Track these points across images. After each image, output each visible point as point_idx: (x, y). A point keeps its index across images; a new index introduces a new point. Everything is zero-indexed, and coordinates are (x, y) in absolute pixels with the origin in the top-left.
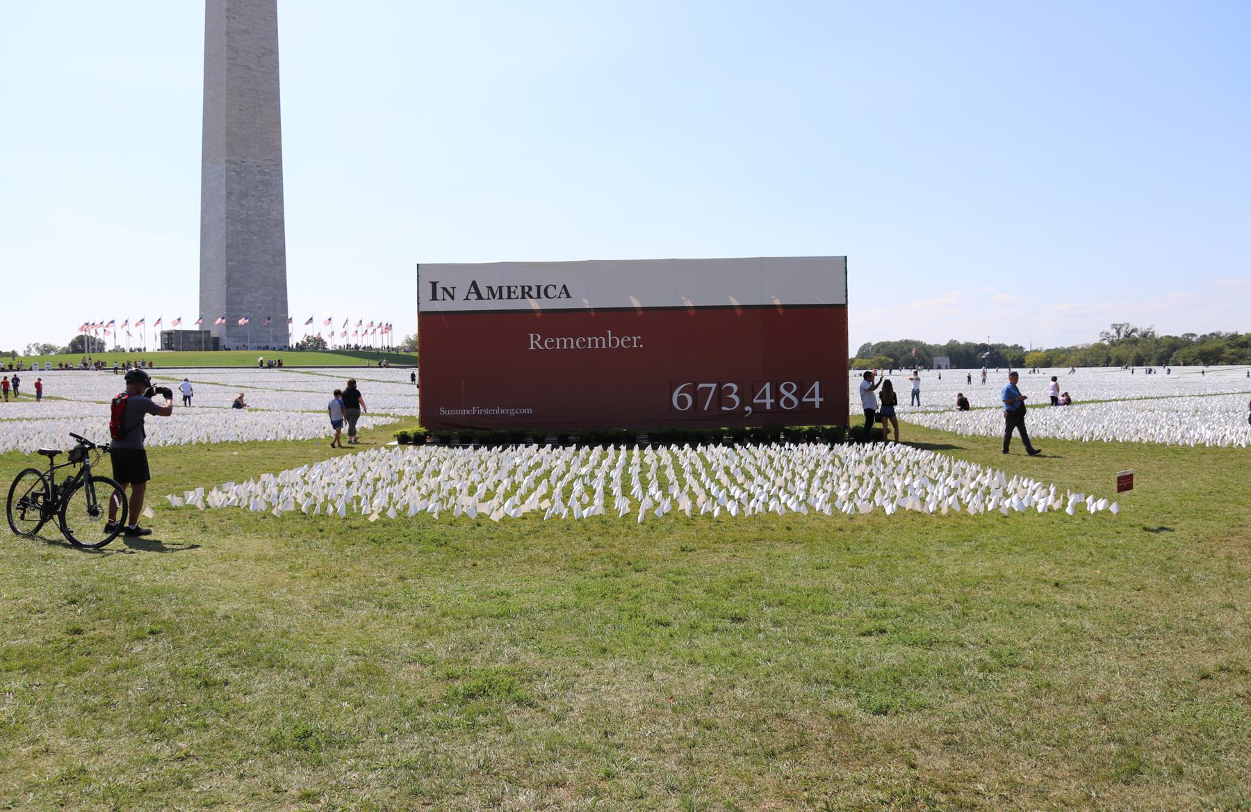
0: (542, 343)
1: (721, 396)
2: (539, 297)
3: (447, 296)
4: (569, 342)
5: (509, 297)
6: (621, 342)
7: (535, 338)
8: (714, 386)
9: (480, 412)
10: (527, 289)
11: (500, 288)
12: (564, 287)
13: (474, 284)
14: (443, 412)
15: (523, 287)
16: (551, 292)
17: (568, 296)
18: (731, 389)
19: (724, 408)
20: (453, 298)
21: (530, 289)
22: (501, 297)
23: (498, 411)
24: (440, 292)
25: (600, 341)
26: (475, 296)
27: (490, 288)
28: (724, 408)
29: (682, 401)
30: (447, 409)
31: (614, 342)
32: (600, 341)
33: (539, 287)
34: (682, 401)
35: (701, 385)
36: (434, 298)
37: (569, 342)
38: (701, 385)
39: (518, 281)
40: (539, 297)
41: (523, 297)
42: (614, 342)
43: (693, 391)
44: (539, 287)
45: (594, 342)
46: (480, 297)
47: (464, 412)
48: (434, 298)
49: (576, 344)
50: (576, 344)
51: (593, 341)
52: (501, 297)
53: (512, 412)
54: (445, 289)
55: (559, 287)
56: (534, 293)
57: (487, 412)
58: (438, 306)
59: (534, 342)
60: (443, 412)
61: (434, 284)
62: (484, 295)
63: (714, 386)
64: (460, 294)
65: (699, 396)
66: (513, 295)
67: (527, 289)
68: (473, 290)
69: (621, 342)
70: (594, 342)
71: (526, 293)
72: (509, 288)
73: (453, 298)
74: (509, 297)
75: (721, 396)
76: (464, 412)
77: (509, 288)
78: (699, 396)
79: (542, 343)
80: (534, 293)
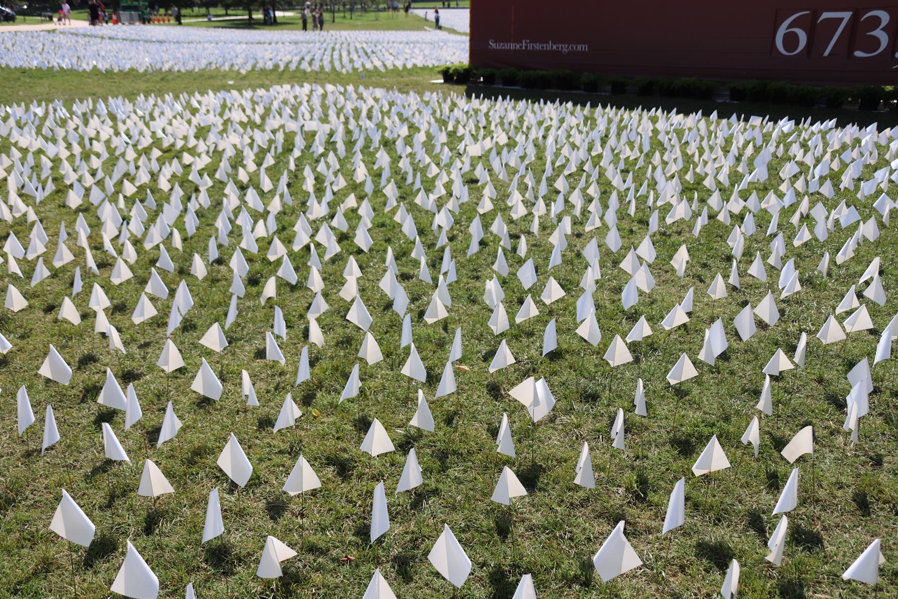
1: (857, 33)
8: (847, 15)
9: (530, 47)
14: (493, 45)
18: (877, 21)
19: (858, 54)
23: (550, 46)
28: (858, 54)
29: (791, 40)
30: (496, 42)
34: (791, 40)
35: (826, 15)
38: (826, 15)
43: (810, 25)
47: (512, 46)
53: (565, 48)
57: (538, 47)
60: (493, 45)
63: (847, 15)
65: (818, 32)
75: (857, 33)
76: (512, 46)
78: (818, 32)
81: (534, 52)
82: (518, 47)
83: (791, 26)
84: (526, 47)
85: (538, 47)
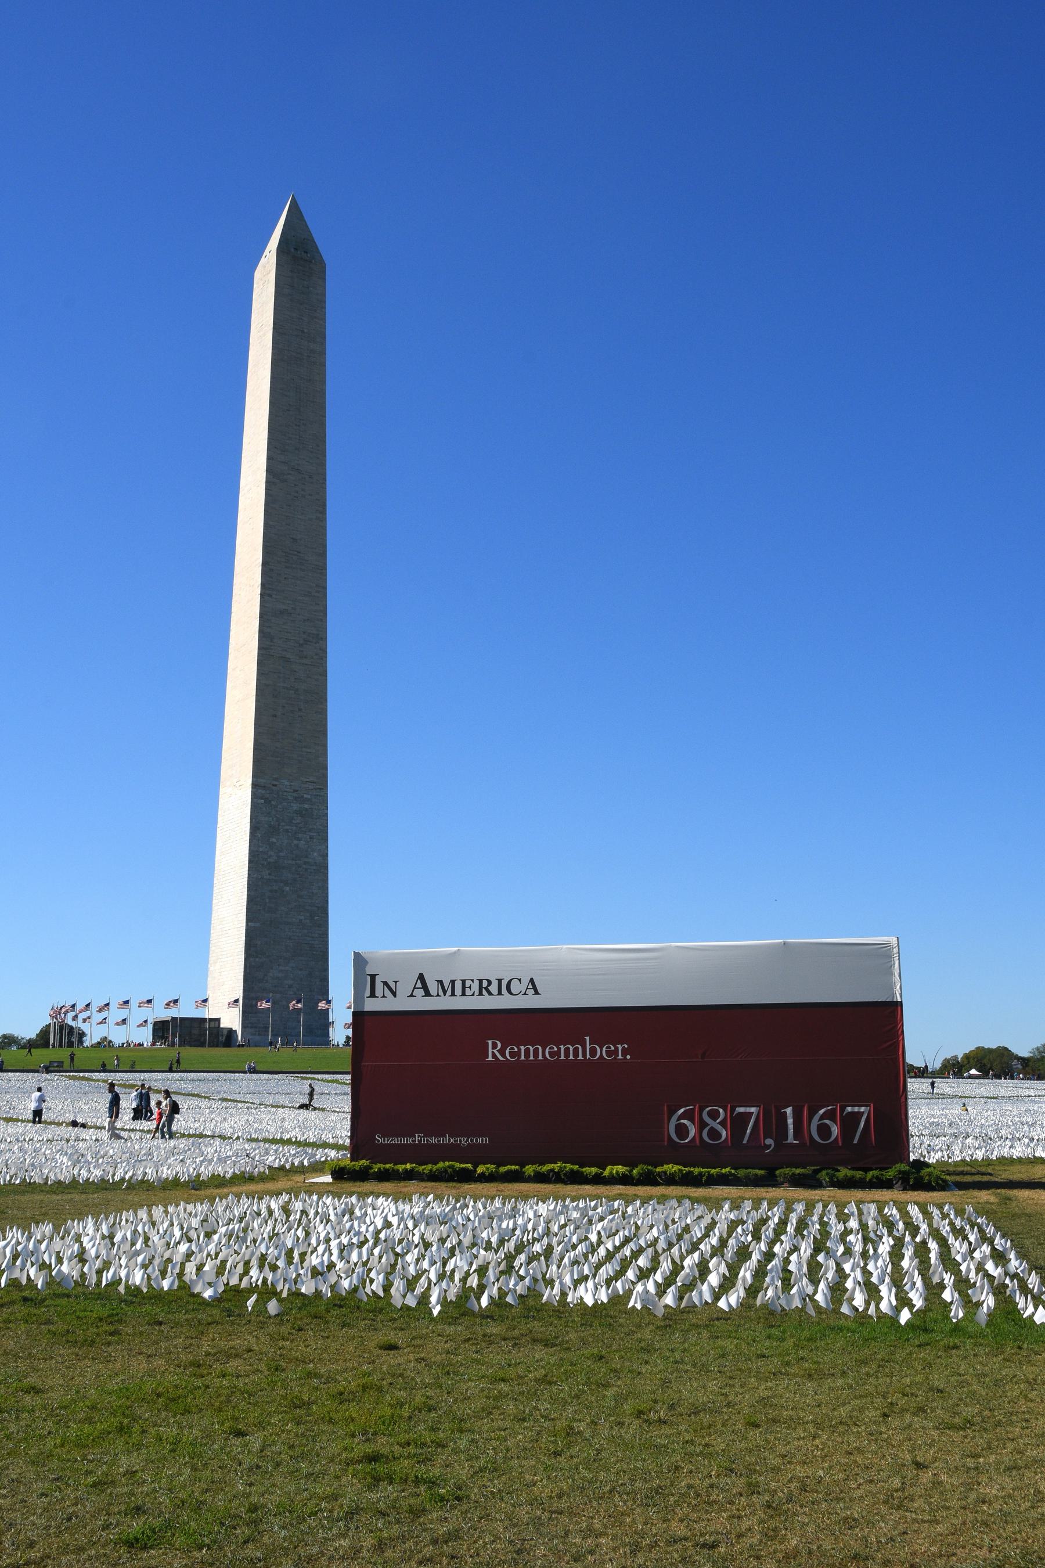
0: (502, 1052)
2: (500, 993)
3: (387, 992)
4: (536, 1051)
5: (464, 994)
6: (602, 1052)
7: (494, 1046)
9: (424, 1140)
10: (485, 984)
11: (453, 982)
12: (532, 981)
13: (421, 977)
15: (481, 981)
16: (514, 988)
17: (537, 993)
20: (394, 994)
21: (489, 982)
22: (453, 994)
24: (379, 986)
25: (576, 1051)
26: (422, 992)
27: (441, 982)
29: (682, 1131)
30: (383, 1136)
31: (593, 1052)
32: (576, 1051)
33: (500, 981)
36: (373, 995)
37: (536, 1051)
39: (474, 974)
40: (500, 993)
41: (481, 994)
42: (593, 1052)
44: (500, 981)
45: (567, 1052)
46: (427, 994)
48: (373, 995)
49: (545, 1053)
50: (545, 1053)
51: (567, 1051)
52: (453, 994)
54: (385, 983)
55: (526, 981)
56: (494, 988)
57: (433, 1140)
58: (371, 1005)
59: (493, 1050)
61: (373, 977)
62: (433, 988)
64: (403, 990)
66: (468, 991)
67: (485, 984)
68: (419, 985)
69: (602, 1052)
70: (567, 1052)
71: (484, 988)
72: (464, 981)
73: (394, 994)
74: (464, 994)
77: (464, 981)
79: (502, 1052)
80: (494, 988)
81: (429, 1146)
82: (410, 1141)
83: (679, 1118)
84: (419, 1141)
85: (433, 1140)
